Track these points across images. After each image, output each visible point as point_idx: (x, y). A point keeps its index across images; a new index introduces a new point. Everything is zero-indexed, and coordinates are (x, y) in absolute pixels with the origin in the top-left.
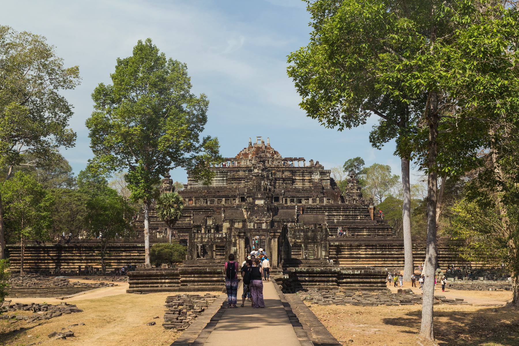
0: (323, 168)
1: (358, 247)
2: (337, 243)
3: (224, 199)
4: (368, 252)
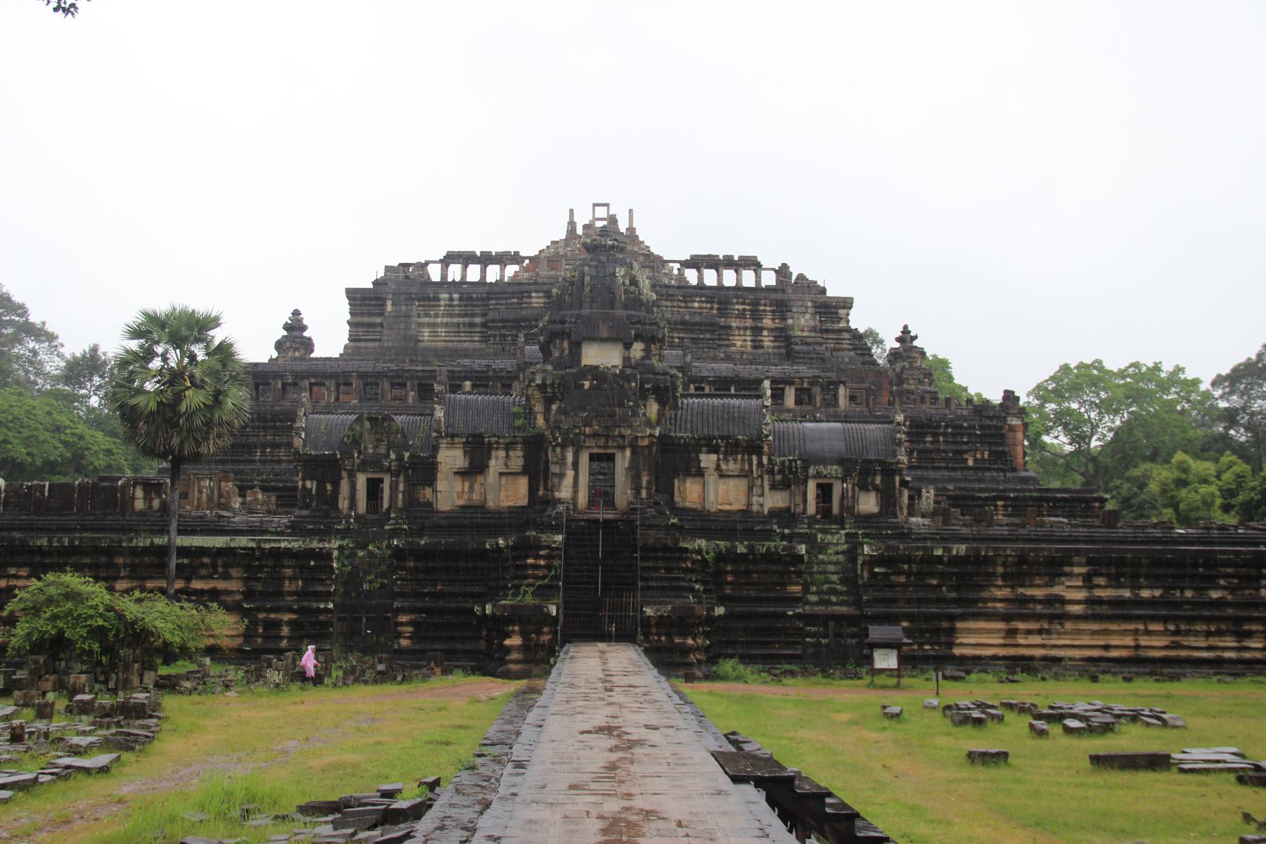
0: (823, 291)
1: (1054, 568)
2: (960, 549)
4: (1099, 593)
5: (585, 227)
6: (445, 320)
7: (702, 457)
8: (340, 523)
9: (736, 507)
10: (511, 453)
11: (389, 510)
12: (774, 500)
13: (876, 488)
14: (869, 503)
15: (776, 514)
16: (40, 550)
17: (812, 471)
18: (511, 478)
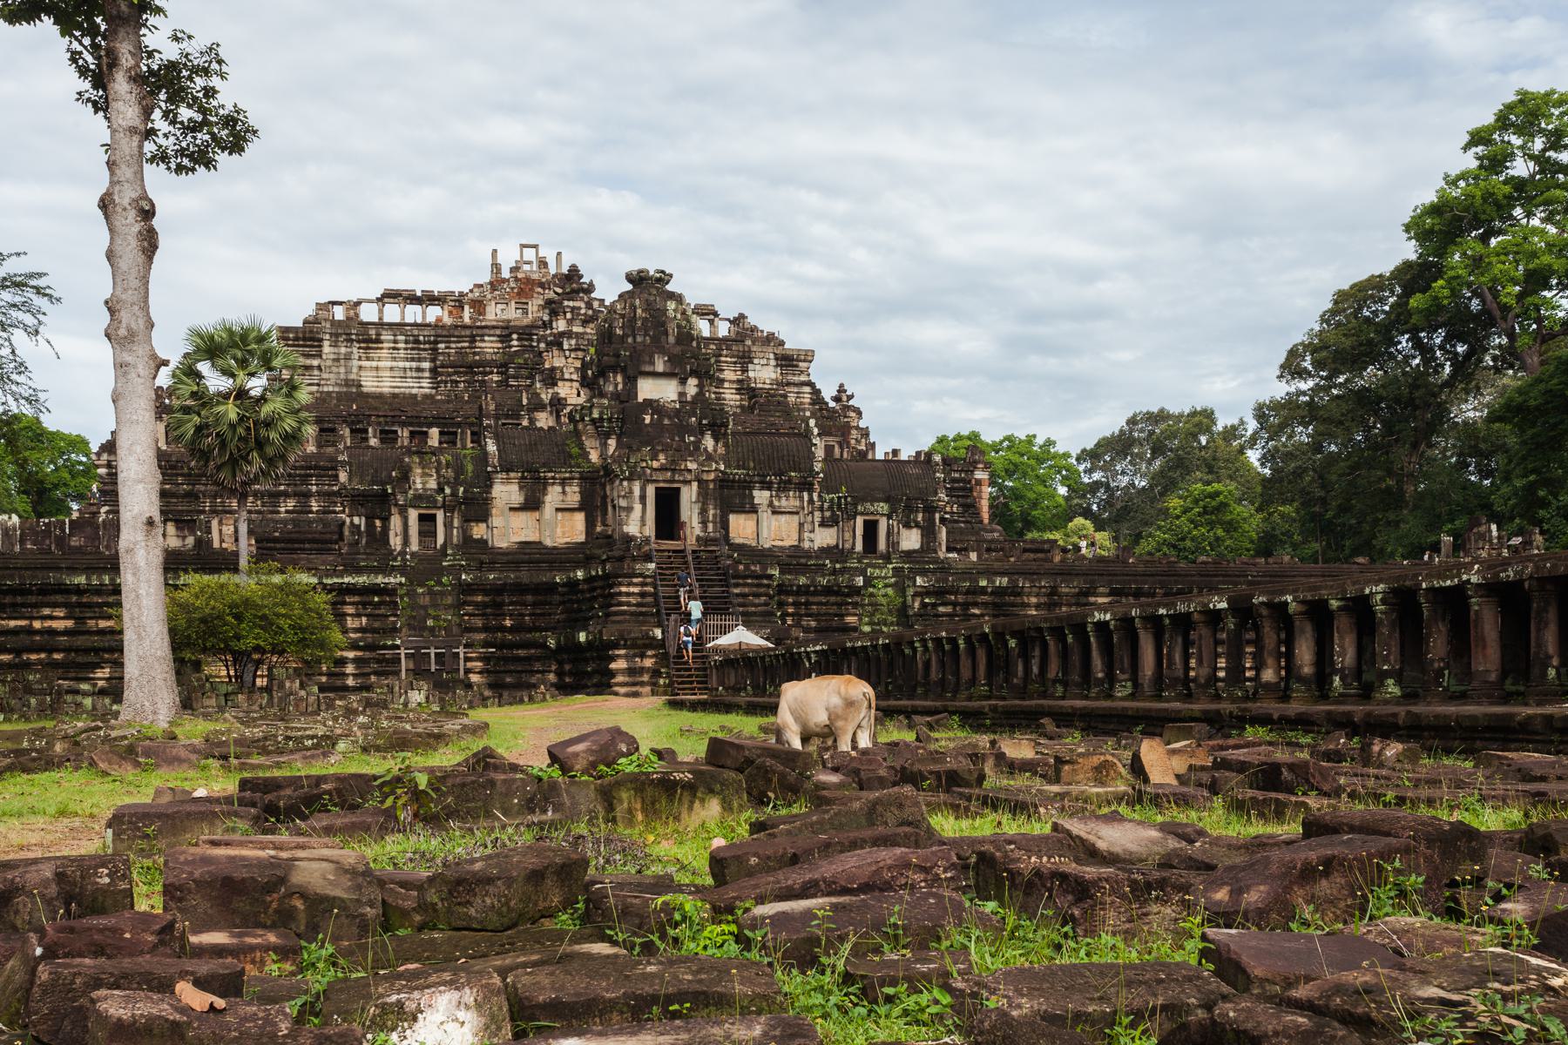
3: (434, 432)
5: (514, 270)
6: (389, 364)
7: (756, 493)
8: (395, 559)
9: (787, 543)
10: (567, 489)
11: (445, 546)
12: (824, 538)
13: (917, 526)
14: (911, 540)
15: (826, 551)
16: (78, 590)
18: (567, 514)
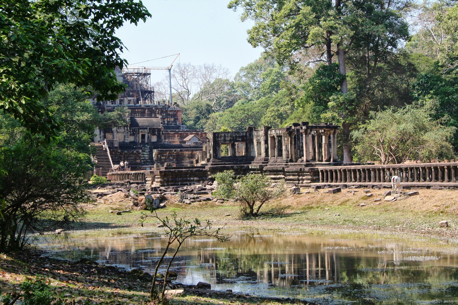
12: (131, 139)
14: (154, 139)
17: (140, 130)
